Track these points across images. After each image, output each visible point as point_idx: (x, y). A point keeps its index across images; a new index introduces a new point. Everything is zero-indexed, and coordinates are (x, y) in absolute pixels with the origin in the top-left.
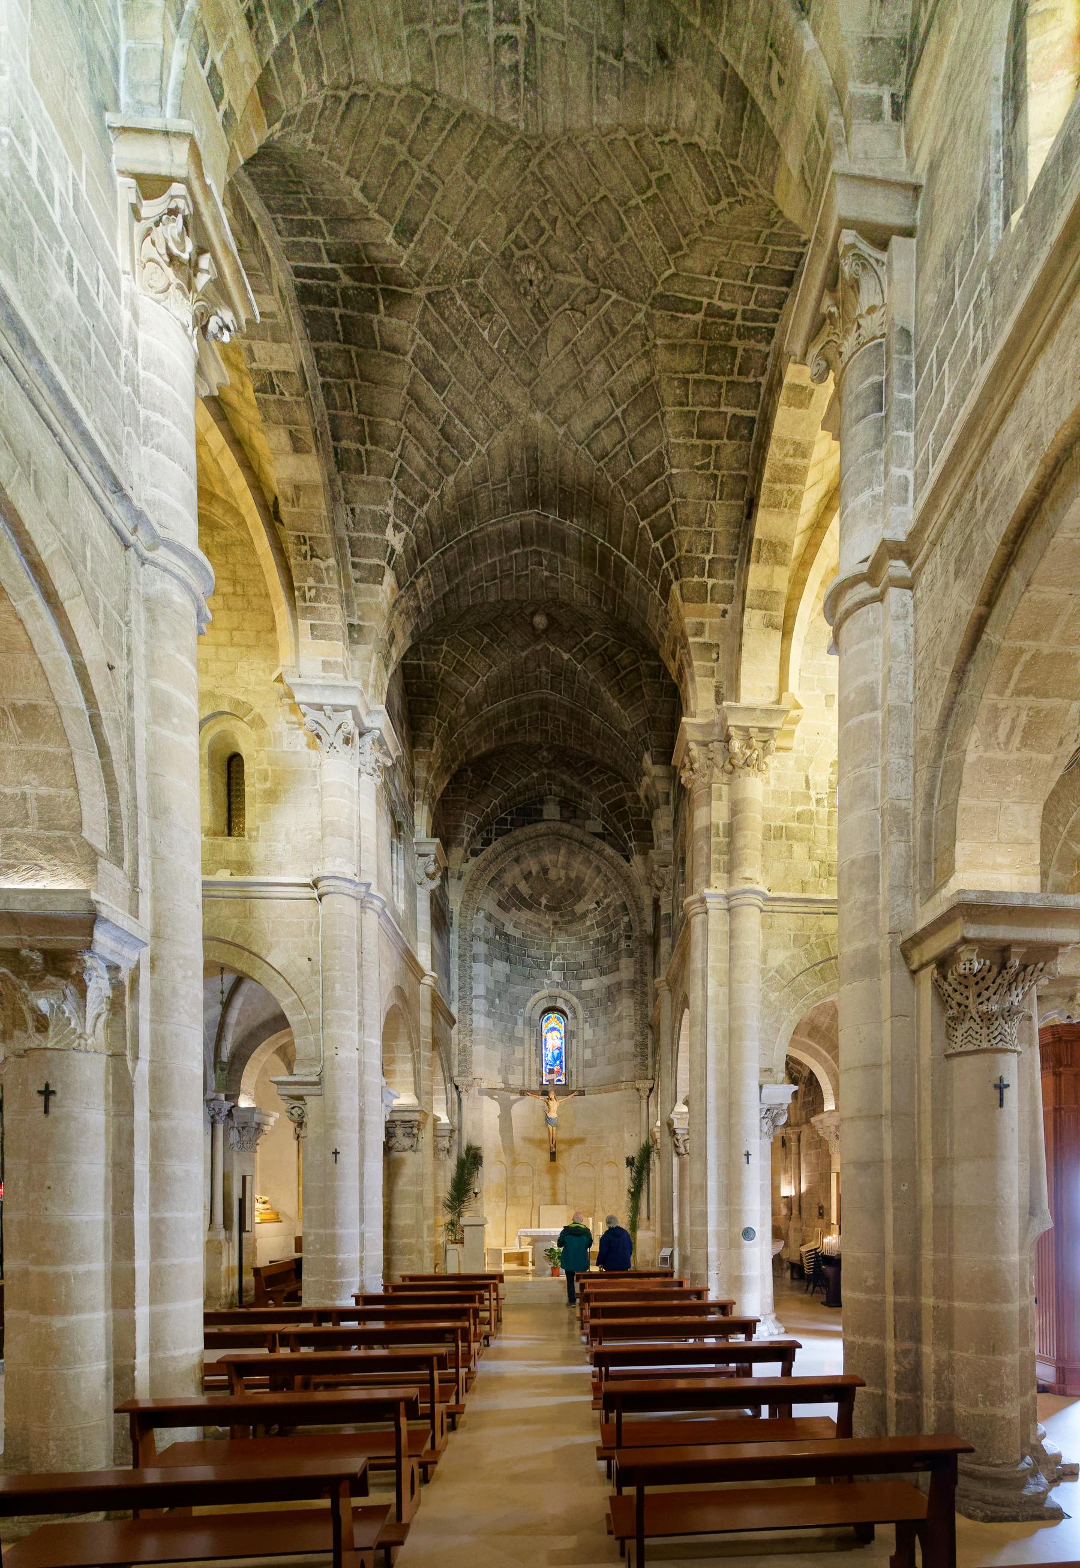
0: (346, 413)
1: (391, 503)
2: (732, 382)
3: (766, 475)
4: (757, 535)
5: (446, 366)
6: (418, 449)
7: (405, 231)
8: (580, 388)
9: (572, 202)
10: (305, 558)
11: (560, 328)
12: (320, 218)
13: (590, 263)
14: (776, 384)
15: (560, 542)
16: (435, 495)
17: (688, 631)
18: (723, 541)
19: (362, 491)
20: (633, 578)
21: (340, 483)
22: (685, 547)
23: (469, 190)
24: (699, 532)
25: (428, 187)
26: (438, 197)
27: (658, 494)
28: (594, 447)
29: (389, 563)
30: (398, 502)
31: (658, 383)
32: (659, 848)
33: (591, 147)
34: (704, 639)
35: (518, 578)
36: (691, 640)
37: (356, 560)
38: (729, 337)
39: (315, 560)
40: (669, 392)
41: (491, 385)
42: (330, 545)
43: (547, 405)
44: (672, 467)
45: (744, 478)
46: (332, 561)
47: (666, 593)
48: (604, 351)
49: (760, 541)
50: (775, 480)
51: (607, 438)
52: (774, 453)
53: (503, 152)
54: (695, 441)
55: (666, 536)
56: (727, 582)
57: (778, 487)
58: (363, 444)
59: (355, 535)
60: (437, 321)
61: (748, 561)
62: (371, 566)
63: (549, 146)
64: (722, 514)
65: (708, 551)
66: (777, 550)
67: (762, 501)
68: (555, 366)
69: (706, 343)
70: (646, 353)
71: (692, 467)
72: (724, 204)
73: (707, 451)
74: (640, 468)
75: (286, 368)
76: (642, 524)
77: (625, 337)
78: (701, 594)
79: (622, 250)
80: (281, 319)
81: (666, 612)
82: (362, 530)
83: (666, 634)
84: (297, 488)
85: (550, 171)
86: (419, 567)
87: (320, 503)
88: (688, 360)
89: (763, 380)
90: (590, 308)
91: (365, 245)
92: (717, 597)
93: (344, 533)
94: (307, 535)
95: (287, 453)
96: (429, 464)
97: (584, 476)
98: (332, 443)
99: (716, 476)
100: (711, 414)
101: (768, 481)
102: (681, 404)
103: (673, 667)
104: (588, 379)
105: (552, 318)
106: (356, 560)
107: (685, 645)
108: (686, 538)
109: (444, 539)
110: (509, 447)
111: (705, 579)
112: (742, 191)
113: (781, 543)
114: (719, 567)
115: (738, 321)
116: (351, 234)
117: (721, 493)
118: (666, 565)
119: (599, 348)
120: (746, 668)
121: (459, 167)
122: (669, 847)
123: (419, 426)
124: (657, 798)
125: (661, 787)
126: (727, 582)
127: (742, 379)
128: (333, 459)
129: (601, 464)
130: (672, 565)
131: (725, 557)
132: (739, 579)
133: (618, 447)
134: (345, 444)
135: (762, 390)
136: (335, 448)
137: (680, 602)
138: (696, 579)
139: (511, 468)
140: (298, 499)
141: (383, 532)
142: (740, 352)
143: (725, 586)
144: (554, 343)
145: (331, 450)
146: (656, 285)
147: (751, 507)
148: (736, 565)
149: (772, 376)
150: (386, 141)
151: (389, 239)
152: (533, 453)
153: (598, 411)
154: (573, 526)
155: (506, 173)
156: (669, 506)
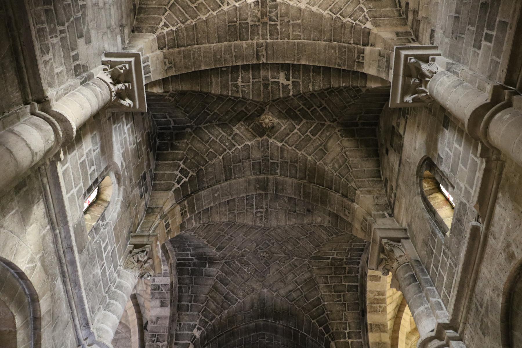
0: (186, 294)
1: (198, 321)
2: (346, 276)
5: (229, 279)
6: (213, 303)
7: (219, 249)
8: (283, 281)
9: (279, 239)
10: (153, 342)
11: (274, 267)
12: (191, 248)
13: (286, 251)
14: (364, 276)
15: (275, 330)
16: (218, 317)
18: (353, 325)
19: (186, 318)
20: (310, 341)
21: (177, 315)
22: (335, 328)
23: (244, 239)
24: (340, 323)
25: (230, 239)
26: (233, 241)
27: (319, 311)
28: (289, 298)
29: (192, 342)
30: (201, 320)
31: (315, 278)
33: (286, 228)
35: (253, 344)
37: (177, 342)
38: (342, 265)
39: (158, 343)
40: (320, 281)
41: (247, 283)
42: (166, 337)
43: (270, 287)
44: (324, 302)
45: (358, 304)
46: (166, 343)
48: (293, 271)
51: (294, 295)
52: (369, 296)
53: (256, 231)
54: (333, 293)
55: (325, 325)
56: (358, 340)
58: (190, 302)
59: (179, 332)
60: (228, 268)
62: (183, 344)
63: (272, 229)
67: (368, 310)
68: (272, 274)
69: (333, 267)
70: (310, 271)
71: (333, 301)
72: (334, 236)
73: (339, 296)
74: (310, 303)
75: (166, 283)
76: (313, 321)
77: (301, 267)
79: (298, 248)
80: (168, 271)
82: (183, 331)
84: (158, 318)
85: (272, 233)
86: (206, 342)
87: (167, 323)
88: (326, 272)
89: (359, 275)
90: (286, 261)
91: (205, 253)
93: (174, 332)
94: (157, 334)
95: (158, 307)
96: (217, 307)
97: (285, 307)
98: (177, 303)
99: (345, 304)
100: (339, 286)
102: (325, 283)
104: (286, 278)
105: (271, 265)
106: (177, 342)
108: (335, 326)
109: (220, 331)
110: (252, 300)
111: (347, 339)
112: (340, 233)
114: (353, 335)
115: (345, 260)
116: (201, 251)
117: (348, 309)
118: (326, 336)
119: (290, 270)
121: (241, 235)
123: (215, 296)
127: (350, 275)
128: (176, 307)
129: (293, 303)
130: (330, 335)
132: (364, 339)
133: (300, 297)
134: (183, 303)
135: (359, 277)
136: (178, 305)
138: (342, 340)
139: (253, 306)
140: (157, 322)
141: (192, 331)
142: (347, 268)
143: (357, 342)
144: (272, 271)
145: (176, 305)
146: (311, 254)
147: (363, 313)
149: (362, 273)
150: (217, 231)
151: (214, 251)
152: (262, 302)
153: (291, 287)
154: (280, 324)
155: (257, 235)
156: (325, 315)
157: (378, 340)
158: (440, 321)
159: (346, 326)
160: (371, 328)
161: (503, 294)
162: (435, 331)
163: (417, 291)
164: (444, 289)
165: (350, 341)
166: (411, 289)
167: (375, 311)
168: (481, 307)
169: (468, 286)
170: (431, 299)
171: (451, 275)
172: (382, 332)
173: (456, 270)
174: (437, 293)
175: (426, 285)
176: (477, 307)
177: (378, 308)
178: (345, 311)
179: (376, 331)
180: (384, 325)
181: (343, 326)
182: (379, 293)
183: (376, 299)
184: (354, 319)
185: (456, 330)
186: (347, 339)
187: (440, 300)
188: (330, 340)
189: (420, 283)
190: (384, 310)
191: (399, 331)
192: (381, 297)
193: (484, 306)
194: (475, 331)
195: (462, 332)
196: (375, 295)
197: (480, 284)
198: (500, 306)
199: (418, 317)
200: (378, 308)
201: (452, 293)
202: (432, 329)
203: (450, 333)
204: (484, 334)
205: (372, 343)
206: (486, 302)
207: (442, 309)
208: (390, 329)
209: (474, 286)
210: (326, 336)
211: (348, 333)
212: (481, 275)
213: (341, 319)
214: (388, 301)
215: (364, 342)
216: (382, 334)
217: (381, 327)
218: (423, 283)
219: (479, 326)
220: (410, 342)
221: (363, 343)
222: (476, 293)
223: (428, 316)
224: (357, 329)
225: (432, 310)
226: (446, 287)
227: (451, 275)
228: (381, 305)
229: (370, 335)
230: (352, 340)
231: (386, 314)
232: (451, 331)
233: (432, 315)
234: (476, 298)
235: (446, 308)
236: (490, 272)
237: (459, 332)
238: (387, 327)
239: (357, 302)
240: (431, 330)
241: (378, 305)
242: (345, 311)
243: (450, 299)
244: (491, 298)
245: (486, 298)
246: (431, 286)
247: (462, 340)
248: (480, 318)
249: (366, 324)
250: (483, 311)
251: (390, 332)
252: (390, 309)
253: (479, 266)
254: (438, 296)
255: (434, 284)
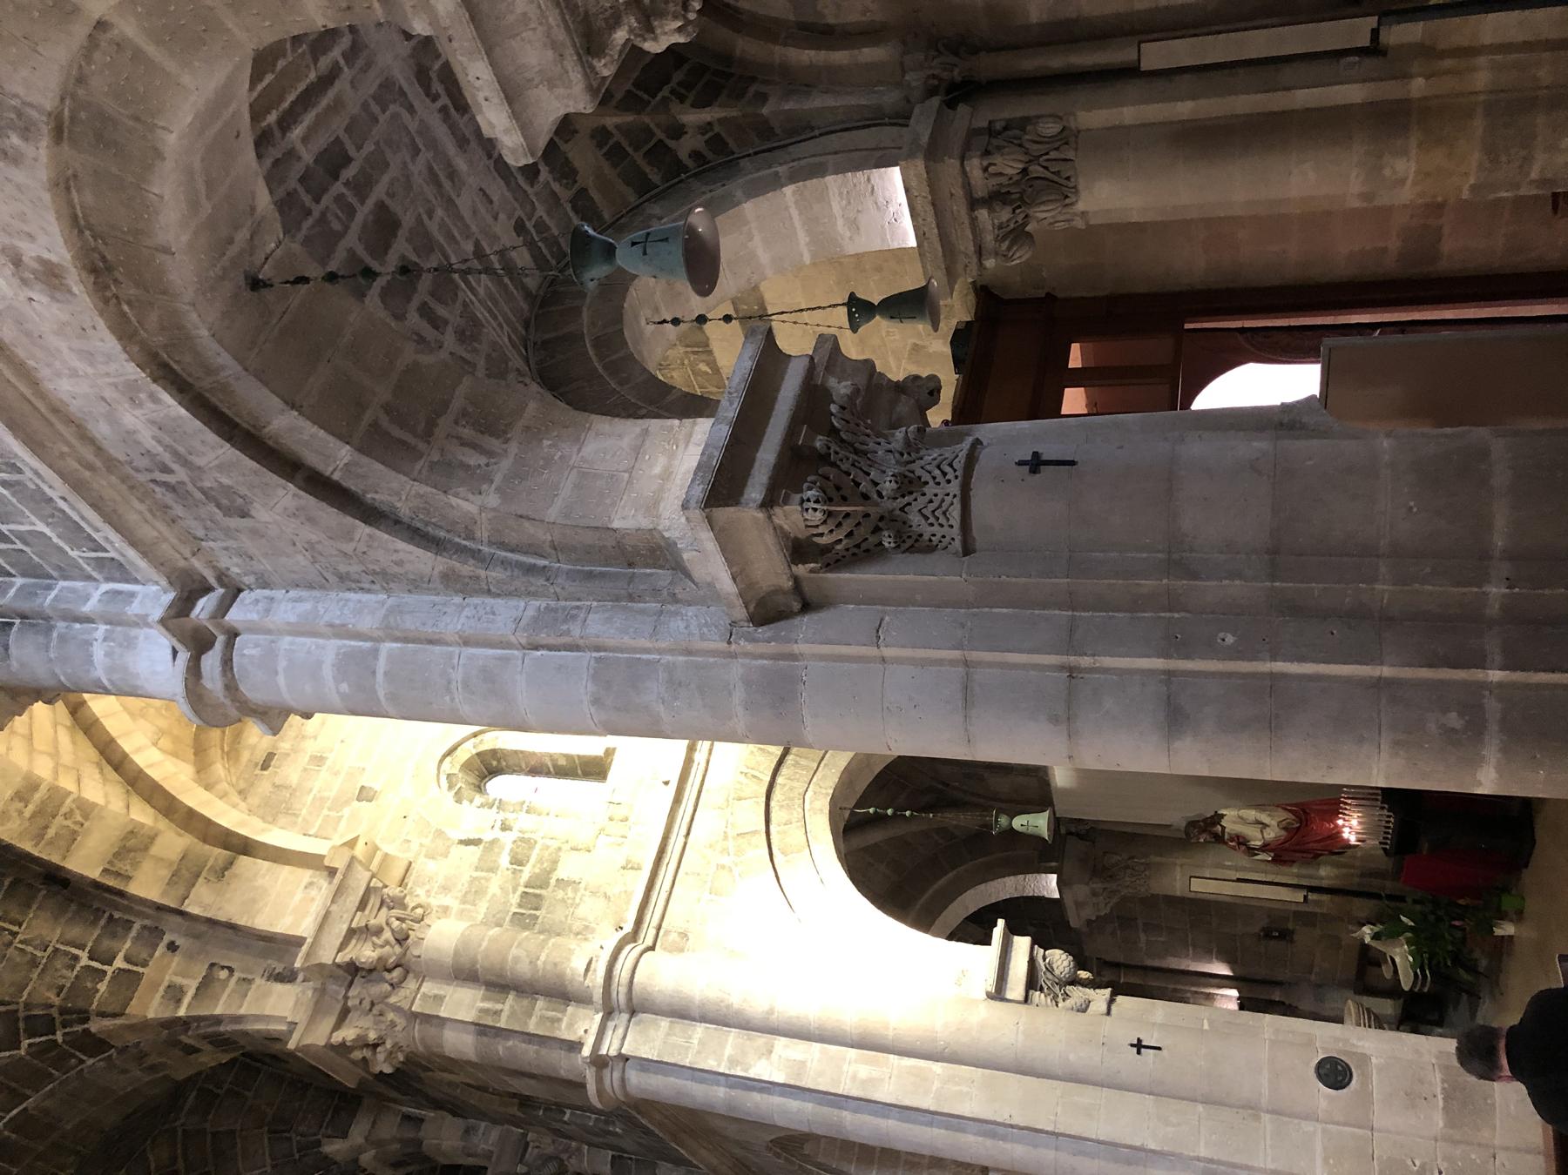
3: (27, 846)
4: (94, 873)
17: (167, 1014)
20: (47, 1103)
32: (488, 1155)
34: (191, 986)
36: (182, 1012)
47: (96, 1045)
49: (105, 871)
50: (40, 836)
55: (21, 1025)
57: (51, 832)
61: (121, 894)
64: (42, 928)
65: (76, 958)
66: (133, 845)
78: (128, 980)
81: (123, 1050)
83: (153, 1059)
92: (144, 955)
101: (36, 845)
103: (209, 1058)
107: (185, 1023)
108: (43, 992)
113: (125, 838)
118: (59, 1037)
120: (262, 923)
122: (495, 1133)
124: (401, 1141)
125: (389, 1128)
126: (133, 933)
131: (97, 932)
137: (118, 1021)
148: (117, 915)
157: (165, 873)
158: (157, 613)
159: (66, 953)
160: (118, 874)
161: (155, 381)
162: (179, 646)
163: (41, 639)
164: (74, 554)
165: (119, 963)
166: (27, 656)
167: (71, 839)
168: (166, 469)
169: (90, 467)
170: (87, 608)
171: (40, 502)
172: (146, 849)
173: (29, 474)
174: (78, 584)
175: (39, 601)
176: (165, 484)
177: (68, 823)
178: (14, 934)
179: (136, 864)
180: (132, 832)
181: (58, 964)
182: (22, 796)
183: (33, 816)
184: (56, 918)
185: (208, 589)
186: (109, 970)
187: (106, 587)
188: (79, 1028)
189: (23, 617)
190: (87, 810)
191: (174, 798)
192: (37, 796)
193: (167, 458)
194: (228, 533)
195: (222, 577)
196: (20, 813)
197: (101, 430)
198: (183, 411)
199: (115, 677)
200: (68, 823)
201: (95, 535)
202: (169, 651)
203: (203, 608)
204: (244, 514)
205: (164, 893)
206: (160, 449)
207: (132, 595)
208: (156, 820)
209: (99, 451)
210: (59, 1037)
211: (91, 958)
212: (75, 407)
213: (34, 962)
214: (67, 783)
215: (147, 917)
216: (154, 850)
217: (132, 843)
218: (25, 606)
219: (219, 515)
220: (224, 786)
221: (147, 922)
222: (122, 458)
223: (130, 644)
224: (94, 923)
225: (120, 624)
226: (75, 545)
227: (40, 502)
228: (64, 810)
229: (134, 889)
230: (121, 955)
231: (102, 808)
232: (201, 603)
233: (134, 632)
234: (137, 470)
235: (136, 581)
236: (74, 374)
237: (212, 581)
238: (143, 825)
239: (7, 883)
240: (170, 657)
241: (59, 820)
242: (14, 934)
243: (112, 554)
244: (153, 422)
245: (147, 437)
246: (49, 588)
247: (240, 591)
248: (199, 495)
249: (96, 885)
250: (181, 474)
251: (163, 824)
252: (99, 790)
253: (42, 395)
254: (89, 585)
255: (51, 577)
